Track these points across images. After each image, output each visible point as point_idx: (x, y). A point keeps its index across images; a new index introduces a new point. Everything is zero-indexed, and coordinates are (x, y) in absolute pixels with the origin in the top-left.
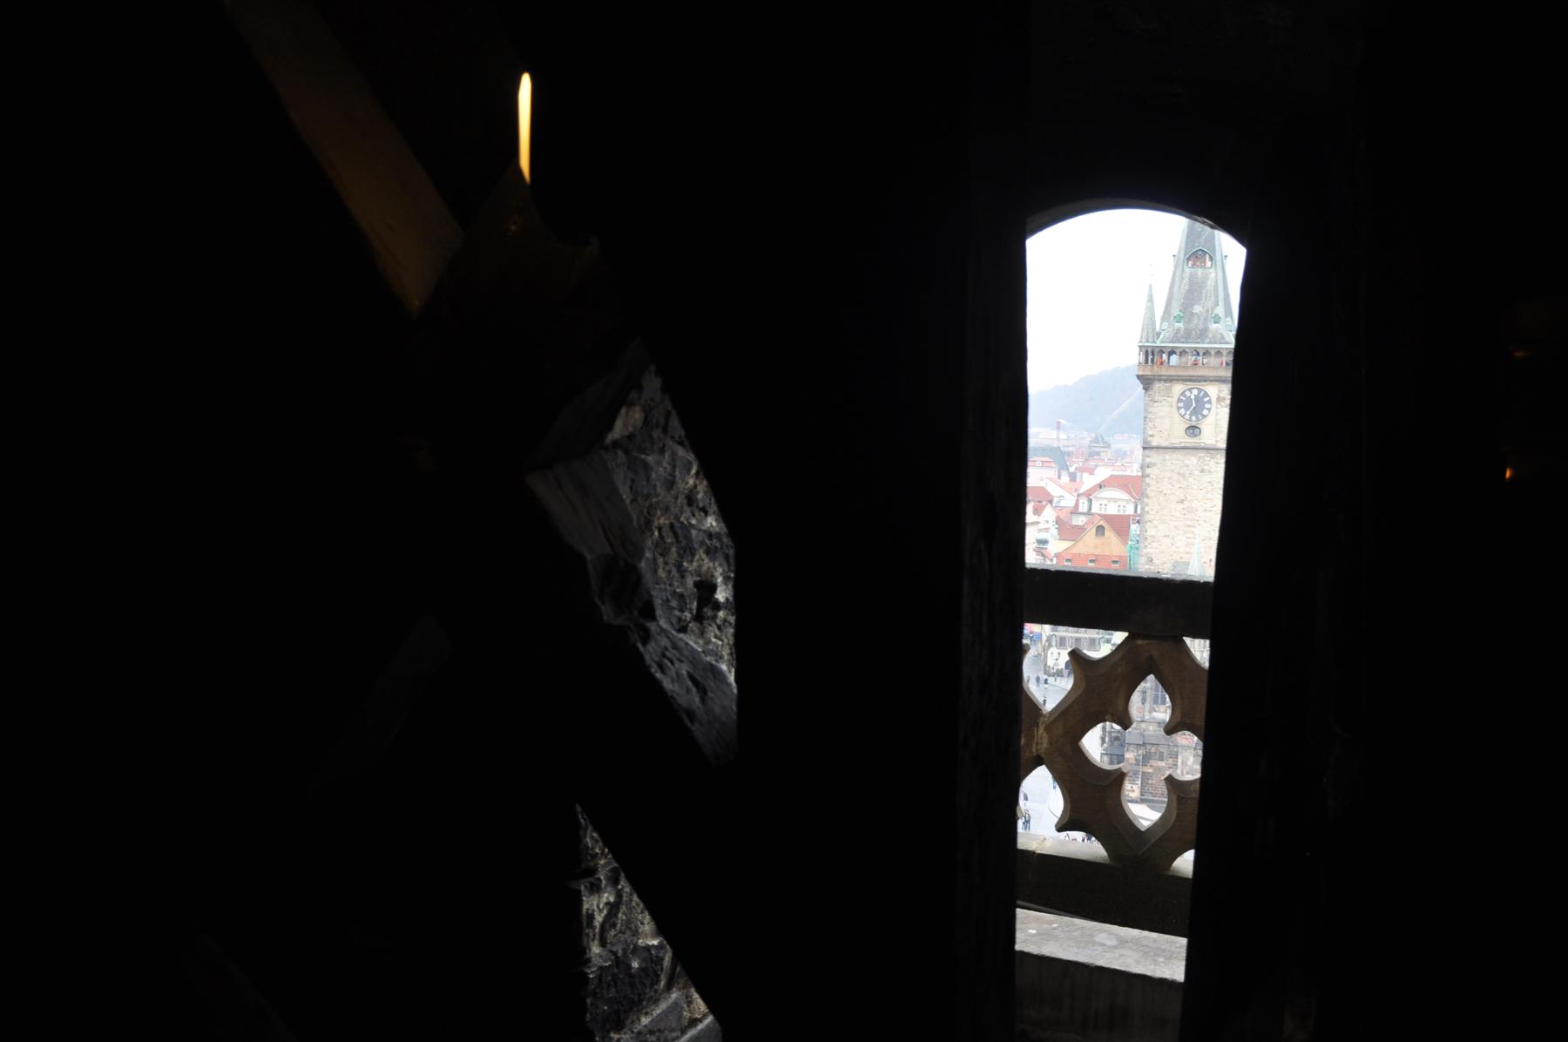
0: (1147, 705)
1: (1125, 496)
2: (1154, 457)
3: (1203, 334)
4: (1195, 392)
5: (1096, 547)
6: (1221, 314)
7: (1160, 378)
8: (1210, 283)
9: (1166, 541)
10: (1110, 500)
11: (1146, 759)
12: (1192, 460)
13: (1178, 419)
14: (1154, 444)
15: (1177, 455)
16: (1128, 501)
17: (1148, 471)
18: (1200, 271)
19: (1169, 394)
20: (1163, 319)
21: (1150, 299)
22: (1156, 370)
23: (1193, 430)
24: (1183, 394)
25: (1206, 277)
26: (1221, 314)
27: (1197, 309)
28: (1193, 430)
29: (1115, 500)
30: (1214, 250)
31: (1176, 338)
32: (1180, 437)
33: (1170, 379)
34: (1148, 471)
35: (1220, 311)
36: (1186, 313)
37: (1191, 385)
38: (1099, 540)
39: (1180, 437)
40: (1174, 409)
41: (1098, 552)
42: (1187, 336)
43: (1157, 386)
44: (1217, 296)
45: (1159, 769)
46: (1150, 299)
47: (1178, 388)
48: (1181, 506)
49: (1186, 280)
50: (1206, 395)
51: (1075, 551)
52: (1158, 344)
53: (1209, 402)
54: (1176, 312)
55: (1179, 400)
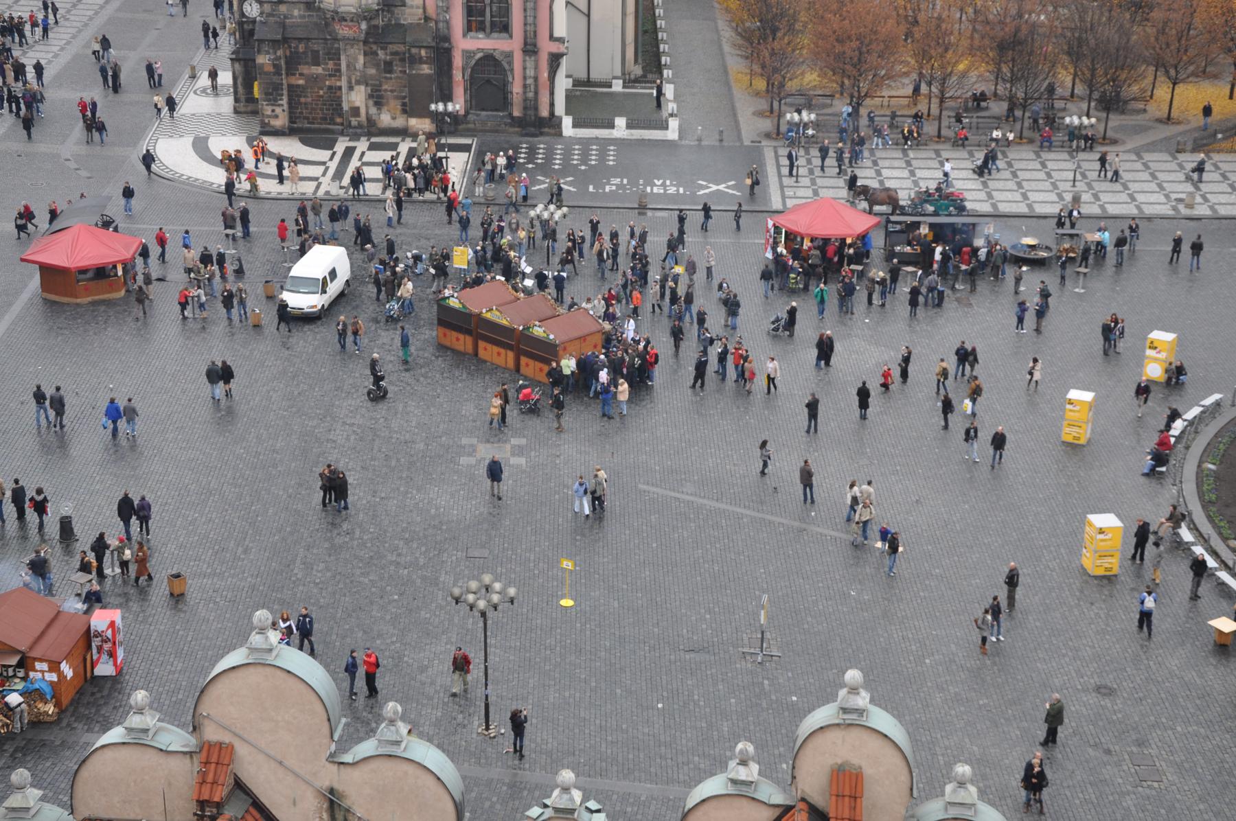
11: (292, 64)
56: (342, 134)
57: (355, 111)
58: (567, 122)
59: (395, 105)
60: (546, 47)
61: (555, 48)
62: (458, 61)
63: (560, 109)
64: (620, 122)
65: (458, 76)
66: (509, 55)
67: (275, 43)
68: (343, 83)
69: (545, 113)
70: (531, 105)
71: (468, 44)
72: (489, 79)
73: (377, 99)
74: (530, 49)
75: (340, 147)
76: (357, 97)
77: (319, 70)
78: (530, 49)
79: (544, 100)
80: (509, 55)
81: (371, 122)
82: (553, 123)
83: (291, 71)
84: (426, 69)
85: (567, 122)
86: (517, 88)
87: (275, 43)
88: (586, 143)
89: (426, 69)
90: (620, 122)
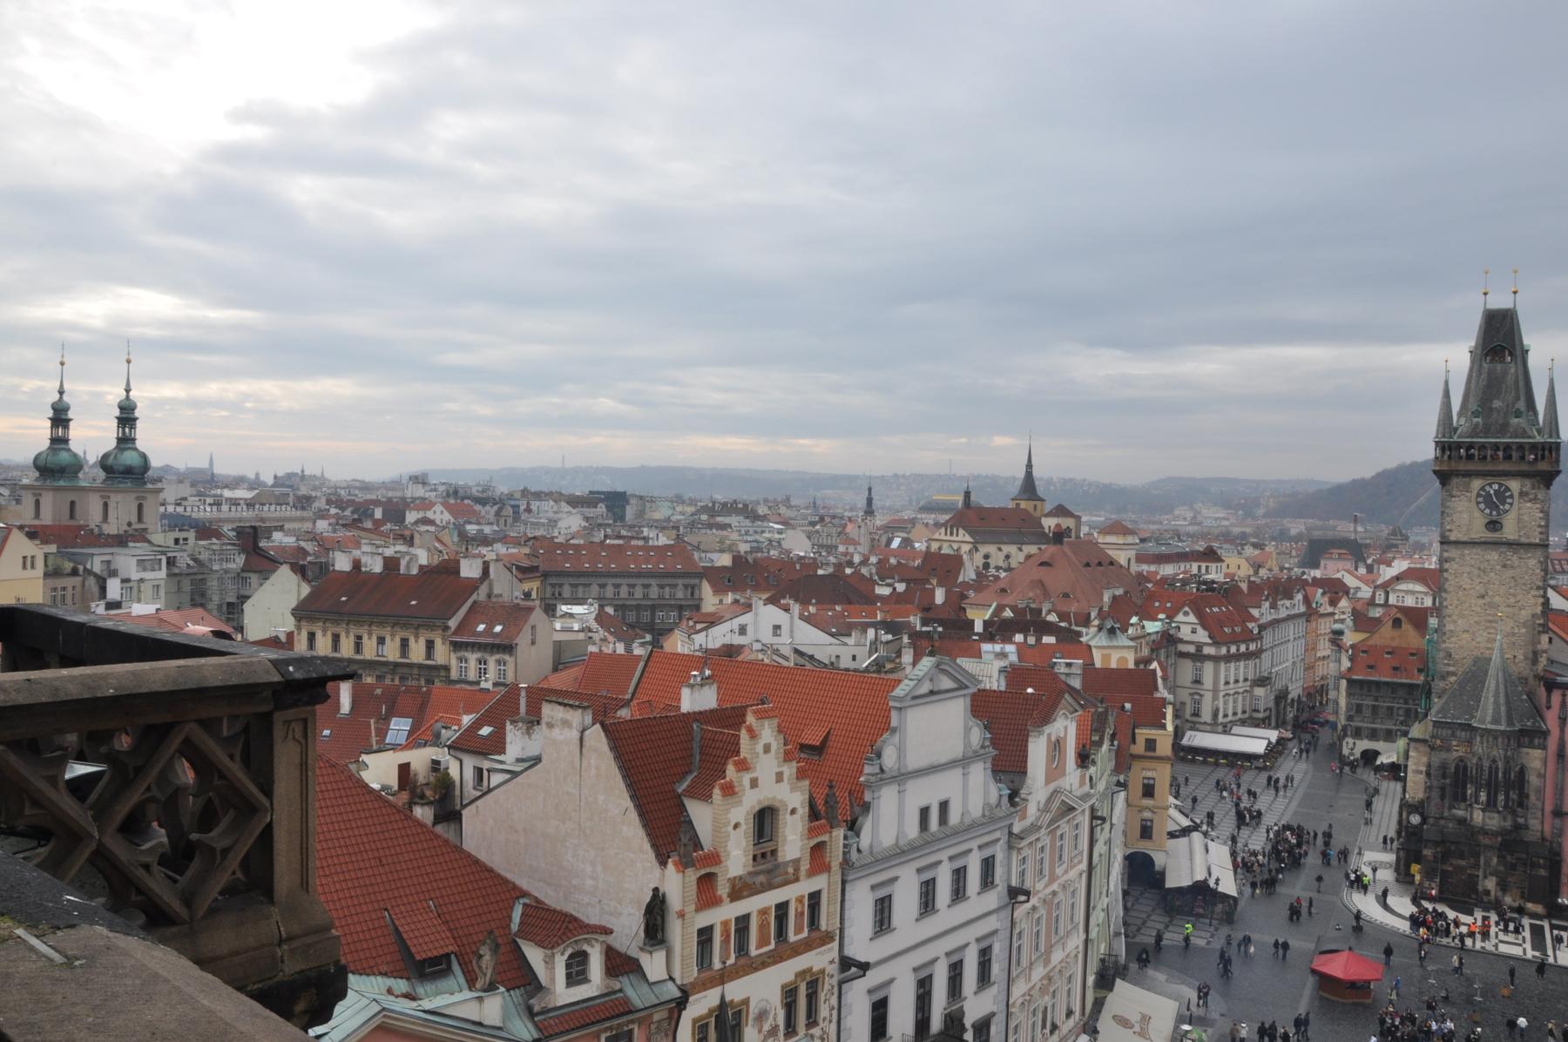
1: (1419, 588)
2: (1453, 552)
3: (1503, 429)
4: (1496, 487)
5: (1393, 639)
7: (1458, 474)
8: (1510, 379)
9: (1465, 636)
10: (1407, 592)
11: (1446, 857)
12: (1493, 556)
13: (1477, 514)
14: (1452, 538)
15: (1478, 550)
16: (1426, 594)
17: (1446, 566)
18: (1499, 367)
19: (1468, 489)
20: (1460, 414)
21: (1447, 394)
22: (1454, 465)
23: (1494, 525)
24: (1483, 489)
25: (1505, 373)
27: (1497, 404)
28: (1494, 525)
29: (1413, 592)
30: (1514, 346)
31: (1474, 432)
32: (1479, 531)
33: (1469, 474)
34: (1446, 566)
35: (1521, 405)
38: (1396, 633)
39: (1479, 531)
40: (1474, 504)
41: (1394, 644)
42: (1486, 431)
43: (1455, 481)
45: (1461, 869)
46: (1447, 394)
47: (1477, 484)
48: (1481, 602)
50: (1508, 489)
51: (1371, 642)
52: (1455, 439)
53: (1511, 496)
54: (1473, 406)
55: (1479, 495)
57: (1487, 892)
67: (1436, 844)
68: (1481, 873)
73: (1503, 886)
76: (1490, 884)
84: (1543, 872)
89: (1543, 872)
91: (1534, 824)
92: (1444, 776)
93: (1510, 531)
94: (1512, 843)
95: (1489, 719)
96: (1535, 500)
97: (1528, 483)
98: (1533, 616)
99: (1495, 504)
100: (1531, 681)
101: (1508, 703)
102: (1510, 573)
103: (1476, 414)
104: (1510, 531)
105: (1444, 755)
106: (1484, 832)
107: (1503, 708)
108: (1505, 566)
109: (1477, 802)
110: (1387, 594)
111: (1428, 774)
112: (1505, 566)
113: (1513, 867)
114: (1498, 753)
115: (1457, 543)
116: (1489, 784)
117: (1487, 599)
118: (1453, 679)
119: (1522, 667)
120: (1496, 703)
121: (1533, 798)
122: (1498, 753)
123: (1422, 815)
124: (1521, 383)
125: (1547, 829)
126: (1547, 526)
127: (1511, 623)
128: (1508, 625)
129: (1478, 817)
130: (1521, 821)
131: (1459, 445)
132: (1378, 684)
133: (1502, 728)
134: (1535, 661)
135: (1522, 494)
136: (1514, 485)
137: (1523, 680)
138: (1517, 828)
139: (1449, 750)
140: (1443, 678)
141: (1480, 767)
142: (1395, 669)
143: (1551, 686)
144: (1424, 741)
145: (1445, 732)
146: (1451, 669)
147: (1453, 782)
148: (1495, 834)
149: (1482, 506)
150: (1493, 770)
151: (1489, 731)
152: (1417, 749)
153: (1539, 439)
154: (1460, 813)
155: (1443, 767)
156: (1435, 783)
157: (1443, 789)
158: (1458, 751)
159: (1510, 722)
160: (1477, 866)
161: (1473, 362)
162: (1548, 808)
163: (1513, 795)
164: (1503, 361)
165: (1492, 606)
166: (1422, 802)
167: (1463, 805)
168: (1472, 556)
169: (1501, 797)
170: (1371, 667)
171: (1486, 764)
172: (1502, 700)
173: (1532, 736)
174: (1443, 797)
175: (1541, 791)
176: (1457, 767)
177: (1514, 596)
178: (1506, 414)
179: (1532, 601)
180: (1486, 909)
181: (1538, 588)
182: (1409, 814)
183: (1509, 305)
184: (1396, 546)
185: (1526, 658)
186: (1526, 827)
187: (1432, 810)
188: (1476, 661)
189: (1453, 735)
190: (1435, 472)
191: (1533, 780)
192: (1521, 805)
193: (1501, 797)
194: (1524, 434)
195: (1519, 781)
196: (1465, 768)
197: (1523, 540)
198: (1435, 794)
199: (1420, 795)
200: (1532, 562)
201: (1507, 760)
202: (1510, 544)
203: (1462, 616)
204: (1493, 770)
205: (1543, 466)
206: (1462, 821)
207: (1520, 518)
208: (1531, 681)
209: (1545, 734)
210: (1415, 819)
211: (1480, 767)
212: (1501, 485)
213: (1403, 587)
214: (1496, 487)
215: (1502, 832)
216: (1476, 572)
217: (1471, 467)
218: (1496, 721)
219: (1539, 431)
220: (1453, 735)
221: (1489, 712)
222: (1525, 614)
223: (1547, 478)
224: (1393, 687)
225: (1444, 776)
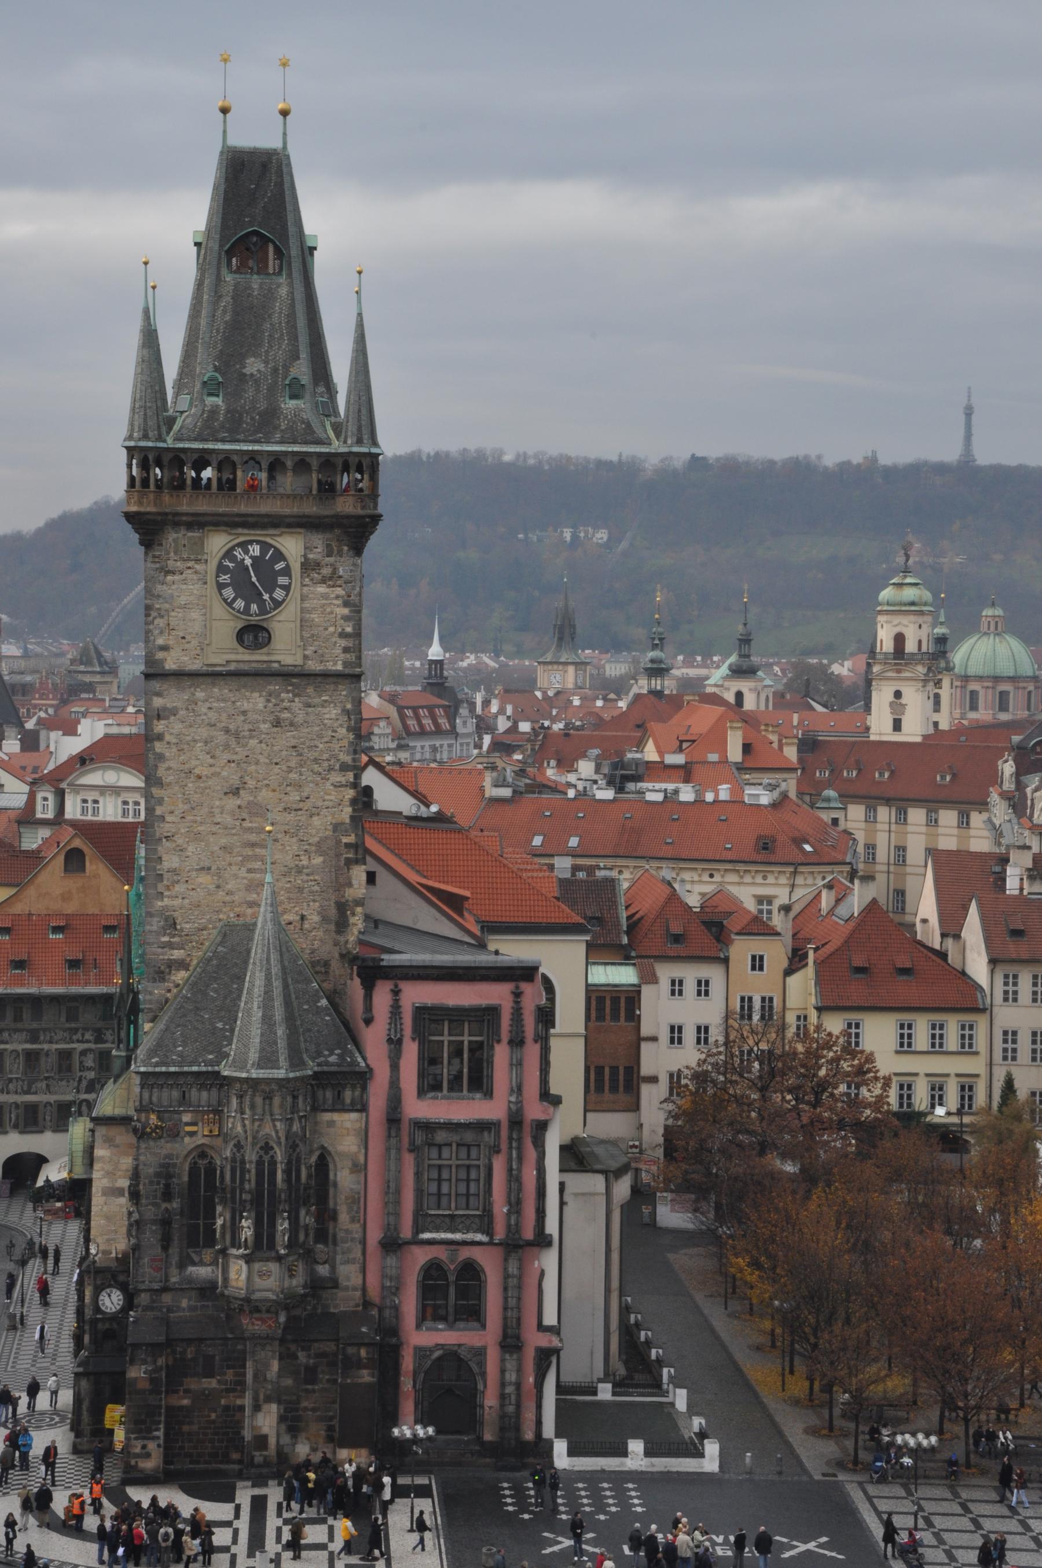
0: (174, 1251)
2: (171, 697)
3: (267, 421)
4: (255, 550)
5: (66, 897)
6: (305, 379)
7: (176, 521)
8: (279, 309)
9: (204, 879)
10: (104, 789)
11: (174, 1377)
12: (254, 701)
13: (219, 610)
14: (170, 665)
17: (159, 727)
21: (150, 339)
22: (170, 502)
23: (253, 635)
24: (229, 554)
25: (269, 295)
26: (305, 379)
27: (253, 366)
28: (253, 635)
29: (116, 790)
32: (223, 649)
33: (200, 523)
34: (159, 727)
35: (302, 370)
36: (227, 377)
37: (244, 535)
38: (73, 883)
39: (223, 649)
40: (211, 588)
41: (70, 908)
42: (234, 428)
43: (172, 537)
44: (294, 338)
46: (150, 339)
47: (217, 543)
48: (232, 802)
49: (226, 301)
50: (279, 556)
51: (18, 908)
52: (170, 442)
53: (287, 572)
54: (205, 369)
55: (221, 569)
56: (240, 1476)
57: (261, 1441)
58: (560, 1447)
59: (318, 1429)
60: (534, 1340)
61: (544, 1341)
62: (408, 1363)
63: (549, 1430)
64: (636, 1446)
65: (407, 1384)
66: (480, 1353)
67: (155, 1349)
68: (247, 1401)
69: (529, 1435)
70: (510, 1423)
71: (422, 1338)
72: (450, 1387)
73: (292, 1422)
74: (511, 1342)
75: (244, 1496)
76: (267, 1421)
77: (212, 1383)
78: (511, 1342)
79: (529, 1415)
80: (480, 1353)
81: (282, 1456)
82: (543, 1449)
83: (172, 1388)
84: (366, 1377)
85: (560, 1447)
86: (490, 1400)
87: (155, 1349)
88: (592, 1478)
89: (366, 1377)
90: (636, 1446)
91: (349, 1274)
92: (167, 1196)
93: (285, 648)
94: (306, 1319)
95: (253, 1056)
96: (330, 580)
97: (318, 541)
98: (336, 827)
99: (254, 586)
100: (336, 966)
101: (290, 1019)
102: (286, 739)
103: (211, 388)
104: (285, 648)
105: (166, 1147)
106: (250, 1305)
107: (281, 1031)
108: (277, 723)
109: (235, 1243)
110: (60, 795)
111: (135, 1195)
112: (277, 723)
113: (310, 1375)
114: (273, 1129)
115: (179, 675)
116: (257, 1200)
117: (245, 797)
118: (180, 976)
119: (315, 940)
120: (267, 1020)
121: (344, 1217)
122: (273, 1129)
123: (123, 1288)
124: (301, 322)
125: (373, 1281)
126: (357, 634)
127: (292, 846)
128: (286, 853)
129: (239, 1274)
130: (323, 1270)
131: (176, 459)
132: (37, 1002)
133: (280, 1073)
134: (342, 926)
135: (308, 566)
136: (292, 546)
137: (320, 967)
138: (317, 1286)
139: (175, 1134)
140: (160, 975)
141: (238, 1164)
142: (74, 964)
143: (372, 973)
144: (123, 1121)
145: (169, 1096)
146: (177, 954)
147: (186, 1206)
148: (272, 1308)
149: (229, 593)
150: (265, 1168)
151: (254, 1084)
152: (109, 1141)
153: (337, 446)
154: (202, 1272)
155: (166, 1172)
156: (150, 1212)
157: (166, 1223)
158: (196, 1134)
159: (296, 1060)
160: (238, 1386)
161: (202, 268)
162: (374, 1235)
163: (307, 1218)
164: (263, 270)
165: (257, 810)
166: (123, 1260)
167: (207, 1255)
168: (211, 703)
169: (283, 1225)
170: (20, 964)
171: (251, 1155)
172: (279, 1014)
173: (337, 1084)
174: (166, 1243)
175: (359, 1201)
176: (194, 1171)
177: (299, 786)
178: (272, 389)
179: (333, 796)
180: (260, 1481)
181: (344, 768)
182: (98, 1291)
183: (276, 144)
184: (90, 688)
185: (325, 919)
186: (334, 1283)
187: (147, 1274)
188: (228, 932)
189: (184, 1099)
190: (129, 517)
191: (344, 1178)
192: (322, 1235)
193: (283, 1225)
194: (309, 436)
195: (313, 1187)
196: (211, 1170)
197: (313, 666)
198: (151, 1236)
199: (121, 1245)
200: (332, 713)
201: (292, 1146)
202: (288, 676)
203: (197, 837)
204: (265, 1168)
205: (346, 506)
206: (207, 1290)
207: (305, 620)
208: (336, 966)
209: (363, 1077)
210: (112, 1301)
211: (238, 1164)
212: (265, 546)
213: (94, 778)
214: (255, 550)
215: (289, 1302)
216: (221, 738)
217: (203, 506)
218: (267, 1060)
219: (337, 429)
220: (184, 1099)
221: (251, 1045)
222: (320, 826)
223: (356, 532)
224: (70, 1005)
225: (167, 1196)
